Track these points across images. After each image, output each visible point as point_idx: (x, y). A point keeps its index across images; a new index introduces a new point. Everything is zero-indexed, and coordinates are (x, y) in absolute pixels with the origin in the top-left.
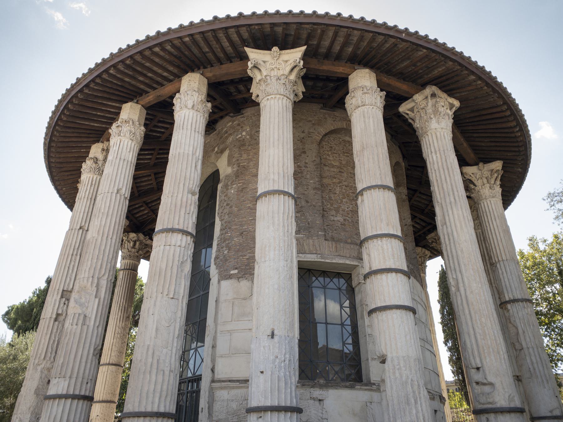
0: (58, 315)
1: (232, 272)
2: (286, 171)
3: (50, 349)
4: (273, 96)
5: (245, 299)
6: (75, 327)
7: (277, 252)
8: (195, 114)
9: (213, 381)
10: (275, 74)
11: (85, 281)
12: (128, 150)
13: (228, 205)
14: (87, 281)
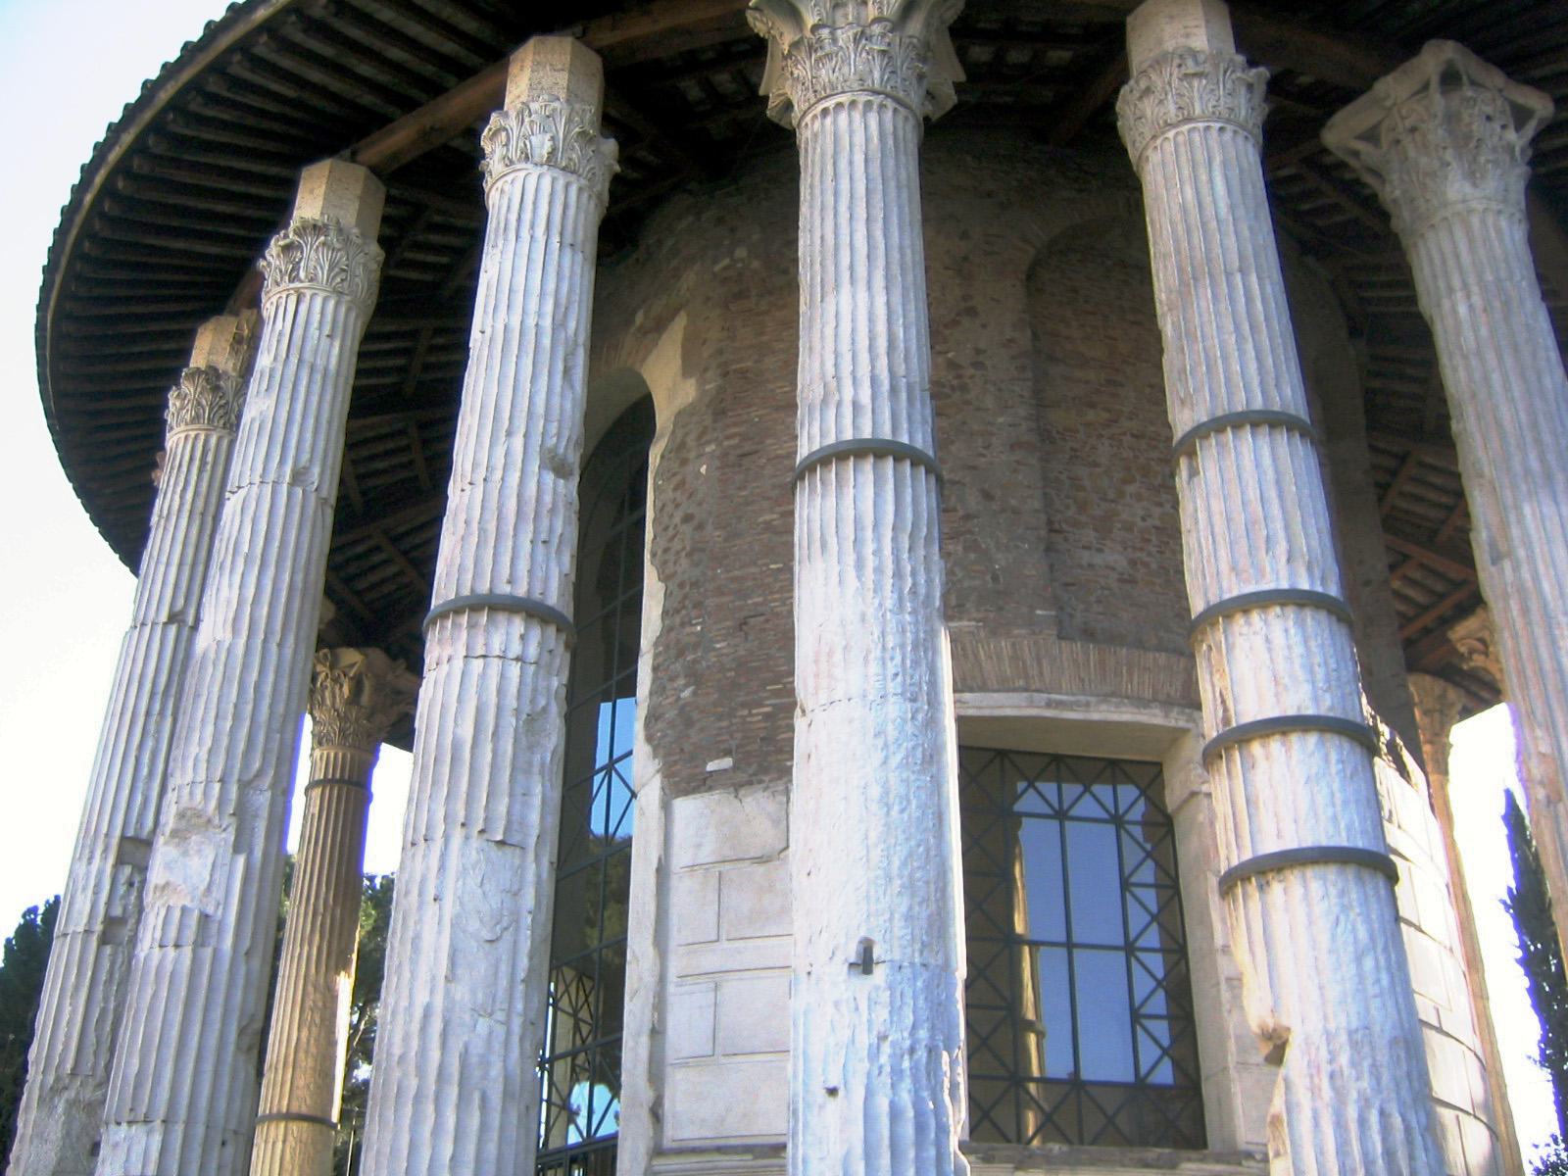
0: (111, 922)
1: (711, 766)
2: (901, 370)
3: (92, 1038)
4: (844, 99)
5: (762, 860)
6: (171, 952)
7: (874, 668)
8: (561, 184)
9: (658, 1151)
11: (199, 790)
12: (327, 331)
13: (688, 518)
14: (205, 794)
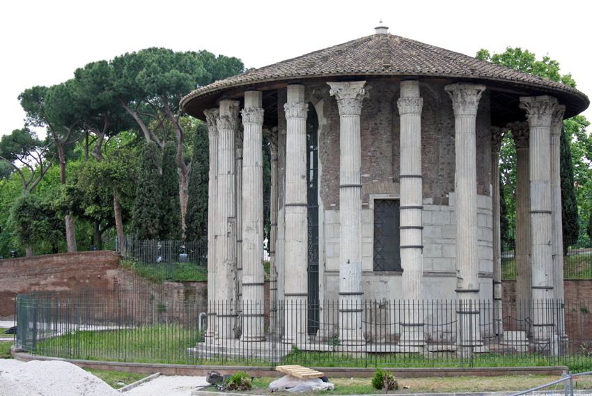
0: (228, 233)
1: (332, 205)
9: (325, 272)
10: (349, 98)
